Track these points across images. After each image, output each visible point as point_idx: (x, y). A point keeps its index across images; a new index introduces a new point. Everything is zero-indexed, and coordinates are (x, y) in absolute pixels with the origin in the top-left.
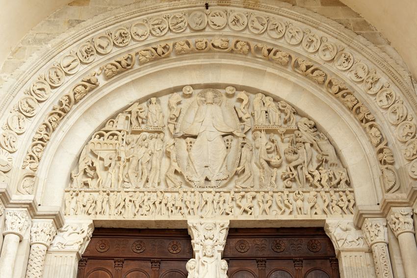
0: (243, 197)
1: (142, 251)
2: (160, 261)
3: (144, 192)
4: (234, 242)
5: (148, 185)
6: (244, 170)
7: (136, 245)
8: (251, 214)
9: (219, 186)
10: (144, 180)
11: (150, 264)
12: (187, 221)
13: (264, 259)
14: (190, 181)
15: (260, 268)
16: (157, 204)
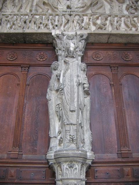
0: (97, 18)
1: (14, 59)
2: (30, 66)
3: (17, 15)
4: (90, 53)
5: (22, 10)
6: (98, 1)
7: (10, 55)
8: (105, 29)
9: (78, 11)
10: (19, 7)
11: (20, 69)
12: (51, 33)
13: (116, 65)
14: (55, 8)
15: (113, 72)
16: (28, 22)
